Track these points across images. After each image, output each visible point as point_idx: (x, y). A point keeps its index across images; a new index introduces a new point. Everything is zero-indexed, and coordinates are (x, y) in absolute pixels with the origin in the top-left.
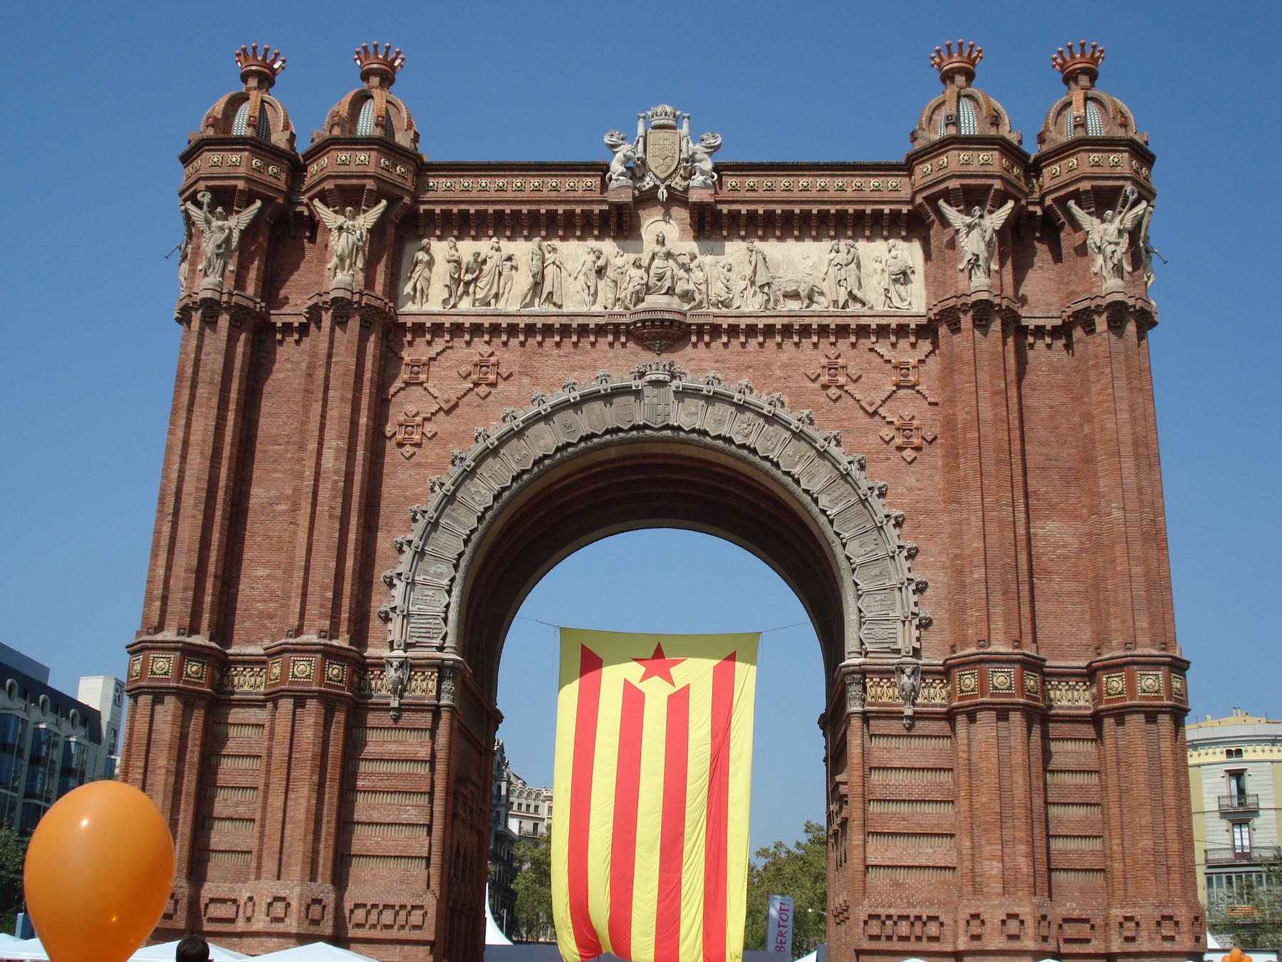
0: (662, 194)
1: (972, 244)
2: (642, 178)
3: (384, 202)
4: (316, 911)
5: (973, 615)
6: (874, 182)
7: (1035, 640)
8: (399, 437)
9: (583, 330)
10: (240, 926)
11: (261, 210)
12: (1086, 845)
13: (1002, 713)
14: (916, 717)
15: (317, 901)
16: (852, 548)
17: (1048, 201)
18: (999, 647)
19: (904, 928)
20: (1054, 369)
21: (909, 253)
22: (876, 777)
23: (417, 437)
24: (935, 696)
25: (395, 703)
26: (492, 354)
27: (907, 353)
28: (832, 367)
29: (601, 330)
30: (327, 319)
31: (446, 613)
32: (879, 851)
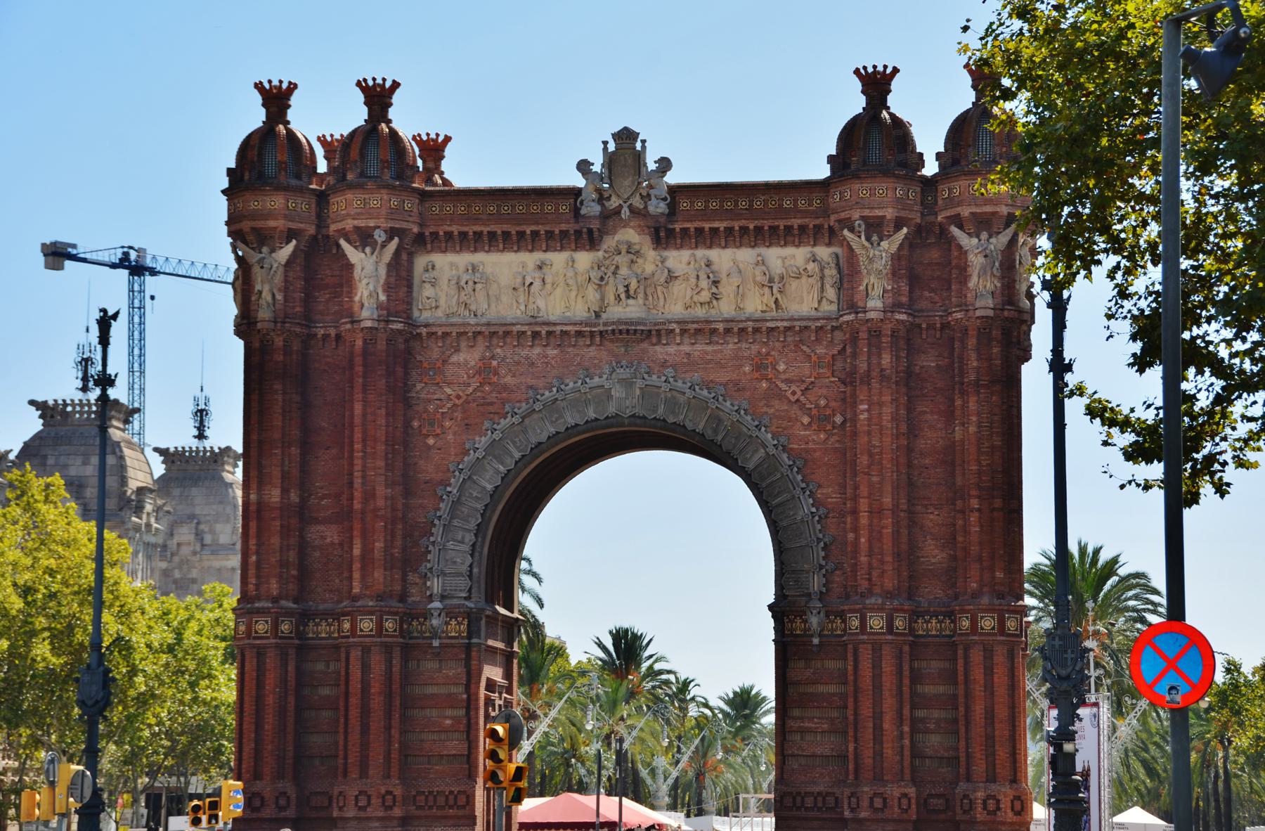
0: (625, 213)
2: (609, 198)
3: (396, 240)
4: (389, 797)
8: (424, 431)
9: (564, 333)
10: (335, 814)
11: (296, 247)
14: (821, 645)
15: (390, 793)
17: (939, 218)
23: (438, 431)
25: (436, 643)
26: (493, 357)
29: (579, 334)
30: (359, 343)
31: (471, 571)
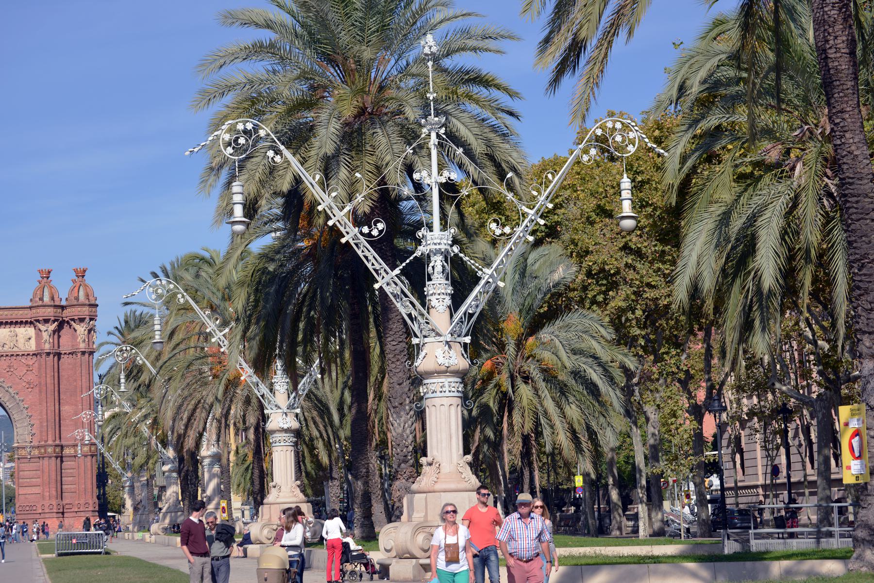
1: (45, 336)
5: (44, 434)
6: (21, 312)
7: (60, 438)
12: (72, 486)
13: (50, 457)
16: (15, 416)
18: (50, 442)
19: (28, 508)
20: (69, 364)
21: (30, 331)
22: (21, 473)
24: (36, 452)
27: (31, 361)
28: (10, 367)
32: (22, 491)
